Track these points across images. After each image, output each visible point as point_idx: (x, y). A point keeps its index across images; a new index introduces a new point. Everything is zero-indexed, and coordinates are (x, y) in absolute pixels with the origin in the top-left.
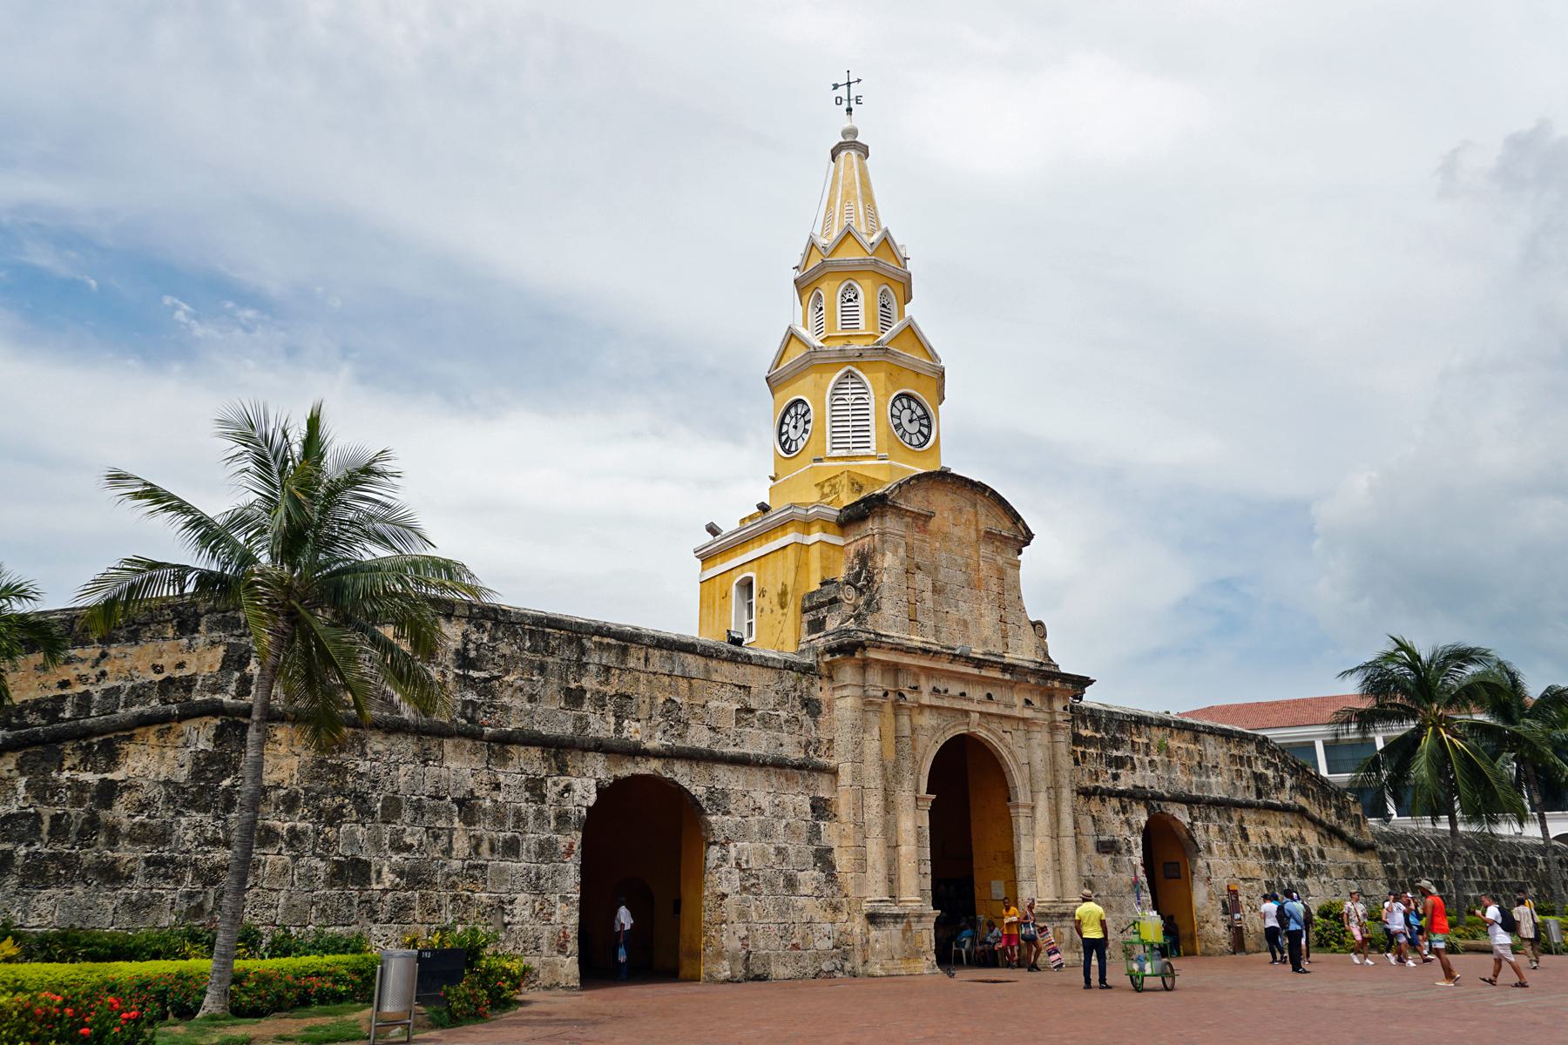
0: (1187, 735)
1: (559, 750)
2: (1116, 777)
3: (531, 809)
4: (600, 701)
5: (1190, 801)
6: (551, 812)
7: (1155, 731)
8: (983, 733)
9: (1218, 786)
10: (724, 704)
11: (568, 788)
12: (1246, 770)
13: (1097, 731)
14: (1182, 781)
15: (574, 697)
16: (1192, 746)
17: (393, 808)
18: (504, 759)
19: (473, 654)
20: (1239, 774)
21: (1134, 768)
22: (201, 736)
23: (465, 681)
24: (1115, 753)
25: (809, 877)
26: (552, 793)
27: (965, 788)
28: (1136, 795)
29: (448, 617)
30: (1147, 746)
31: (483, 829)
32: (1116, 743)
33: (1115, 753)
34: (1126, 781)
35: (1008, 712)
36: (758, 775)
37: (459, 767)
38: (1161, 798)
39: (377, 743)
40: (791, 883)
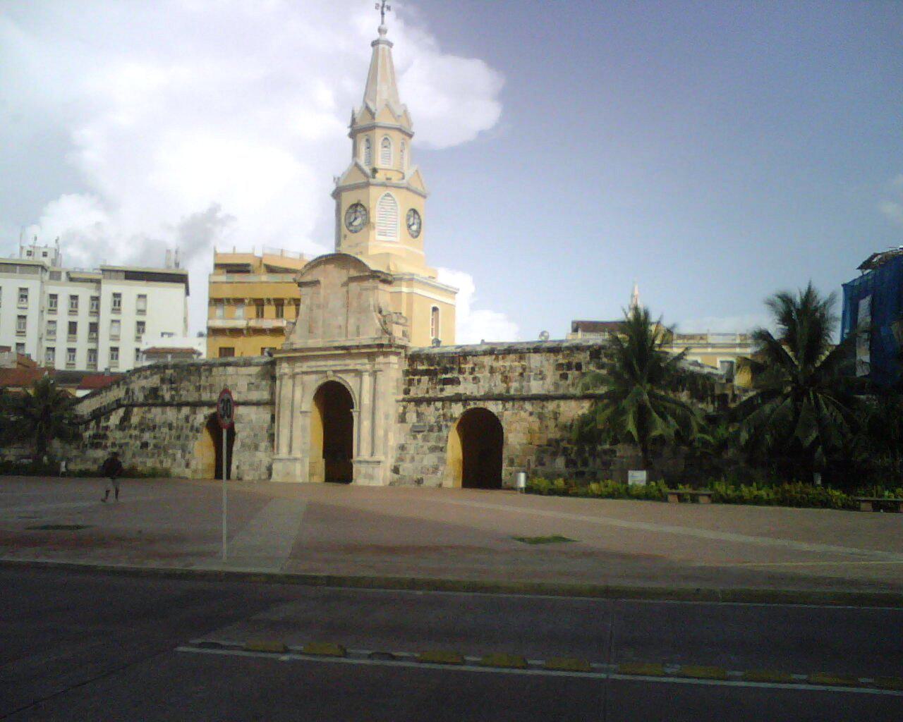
0: (512, 356)
1: (196, 405)
2: (442, 390)
3: (185, 425)
4: (205, 388)
5: (503, 398)
6: (189, 425)
7: (481, 359)
8: (337, 380)
9: (536, 387)
10: (242, 384)
11: (195, 418)
12: (573, 374)
13: (432, 365)
14: (500, 388)
15: (198, 388)
16: (517, 364)
17: (154, 427)
18: (179, 411)
19: (173, 379)
20: (564, 377)
21: (459, 383)
22: (121, 412)
23: (172, 389)
24: (444, 376)
25: (264, 444)
26: (191, 419)
27: (336, 406)
28: (457, 398)
29: (167, 369)
30: (473, 369)
31: (173, 432)
32: (446, 371)
33: (444, 376)
34: (450, 391)
35: (346, 368)
36: (254, 409)
37: (171, 414)
38: (475, 399)
39: (154, 410)
40: (256, 448)
